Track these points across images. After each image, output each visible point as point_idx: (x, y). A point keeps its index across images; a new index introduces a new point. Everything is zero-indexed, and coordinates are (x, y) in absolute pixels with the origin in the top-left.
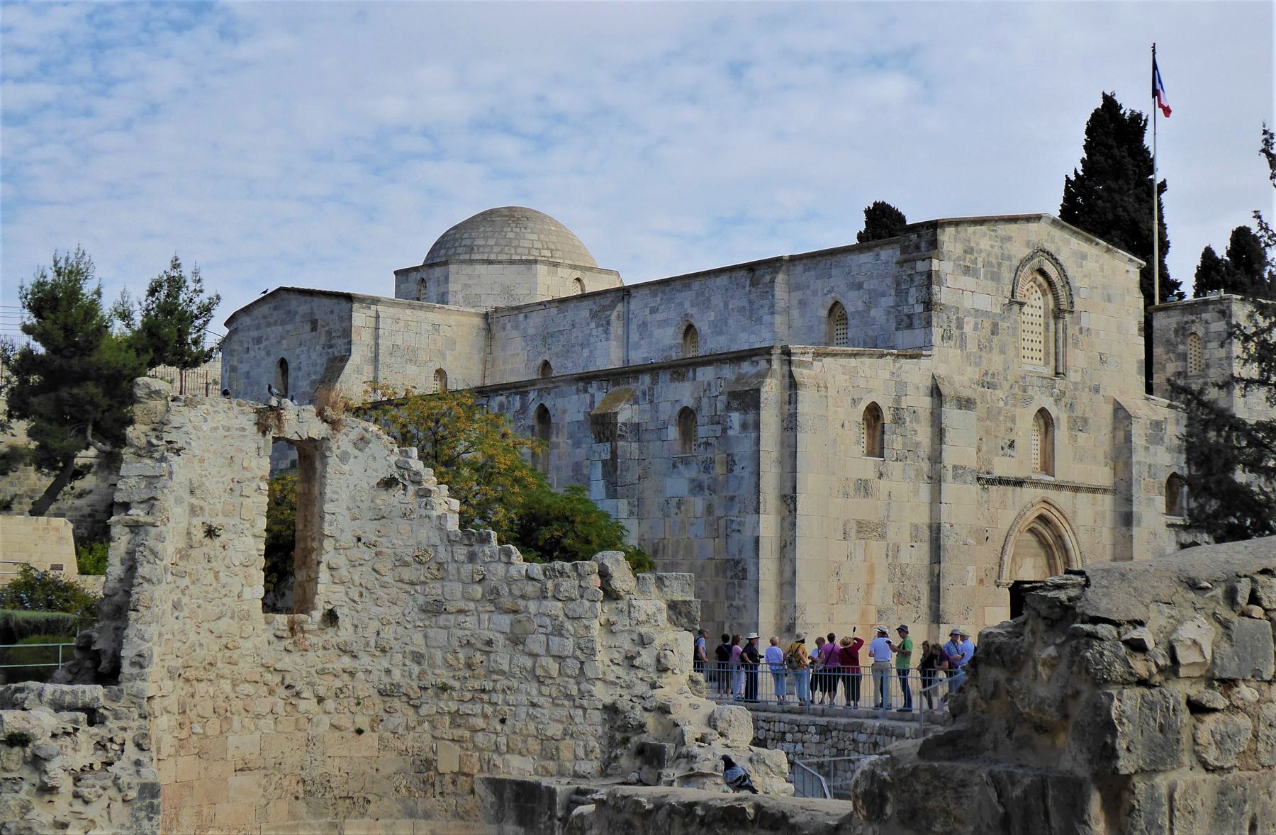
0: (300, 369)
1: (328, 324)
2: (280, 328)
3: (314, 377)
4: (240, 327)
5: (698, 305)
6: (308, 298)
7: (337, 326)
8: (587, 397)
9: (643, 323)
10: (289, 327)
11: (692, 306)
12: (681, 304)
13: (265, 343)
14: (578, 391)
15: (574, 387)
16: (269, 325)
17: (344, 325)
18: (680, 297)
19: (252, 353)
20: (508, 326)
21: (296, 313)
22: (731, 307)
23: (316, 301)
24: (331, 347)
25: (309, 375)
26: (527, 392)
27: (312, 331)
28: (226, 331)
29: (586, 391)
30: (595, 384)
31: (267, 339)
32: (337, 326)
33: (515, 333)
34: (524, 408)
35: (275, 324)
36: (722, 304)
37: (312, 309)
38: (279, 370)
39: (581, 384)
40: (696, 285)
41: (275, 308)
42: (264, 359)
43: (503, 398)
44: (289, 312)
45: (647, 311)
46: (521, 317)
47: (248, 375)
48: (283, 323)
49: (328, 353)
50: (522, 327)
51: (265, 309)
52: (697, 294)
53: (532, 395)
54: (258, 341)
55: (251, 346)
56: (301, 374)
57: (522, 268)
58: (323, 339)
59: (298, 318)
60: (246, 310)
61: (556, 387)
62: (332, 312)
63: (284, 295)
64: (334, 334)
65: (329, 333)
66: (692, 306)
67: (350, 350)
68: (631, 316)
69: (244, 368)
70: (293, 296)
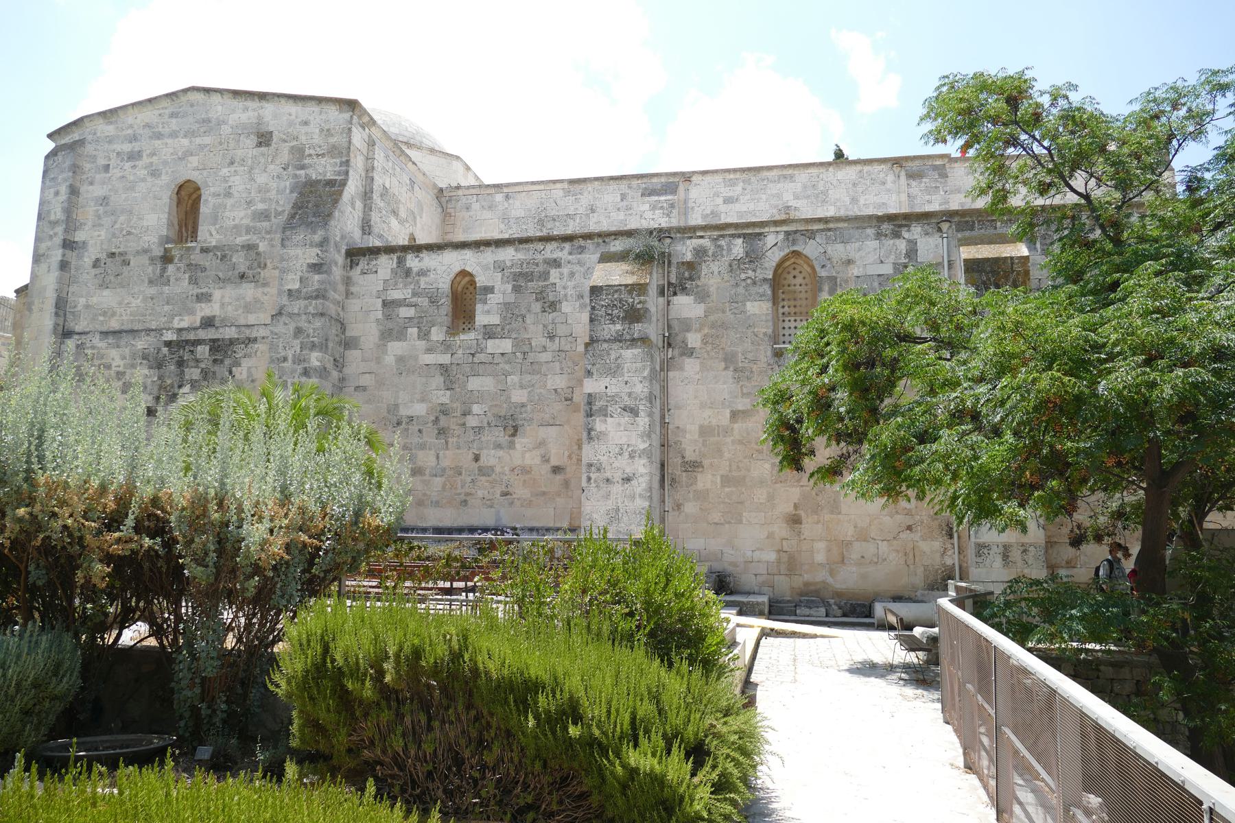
0: (228, 194)
1: (296, 138)
2: (185, 142)
3: (261, 206)
4: (89, 138)
5: (808, 197)
6: (253, 104)
7: (317, 140)
8: (902, 245)
9: (712, 213)
10: (207, 140)
11: (796, 197)
12: (779, 196)
13: (146, 160)
14: (879, 236)
15: (870, 231)
16: (159, 136)
17: (332, 140)
18: (774, 189)
19: (115, 173)
20: (476, 206)
21: (220, 123)
22: (862, 201)
23: (268, 109)
24: (303, 167)
25: (249, 203)
26: (760, 234)
27: (260, 144)
28: (51, 145)
29: (897, 235)
30: (916, 231)
31: (153, 154)
32: (317, 140)
33: (487, 214)
34: (753, 257)
35: (174, 135)
36: (847, 200)
37: (260, 118)
38: (175, 197)
39: (886, 227)
40: (802, 177)
41: (173, 115)
42: (143, 180)
43: (705, 242)
44: (207, 121)
45: (720, 201)
46: (499, 197)
47: (104, 200)
48: (190, 134)
49: (296, 176)
50: (500, 208)
51: (148, 115)
52: (805, 187)
53: (771, 240)
54: (134, 156)
55: (112, 163)
56: (230, 202)
57: (443, 161)
58: (285, 156)
59: (226, 130)
60: (108, 115)
61: (829, 230)
62: (306, 123)
63: (200, 97)
64: (307, 152)
65: (299, 152)
66: (796, 197)
67: (347, 173)
68: (691, 204)
69: (97, 191)
70: (216, 98)
